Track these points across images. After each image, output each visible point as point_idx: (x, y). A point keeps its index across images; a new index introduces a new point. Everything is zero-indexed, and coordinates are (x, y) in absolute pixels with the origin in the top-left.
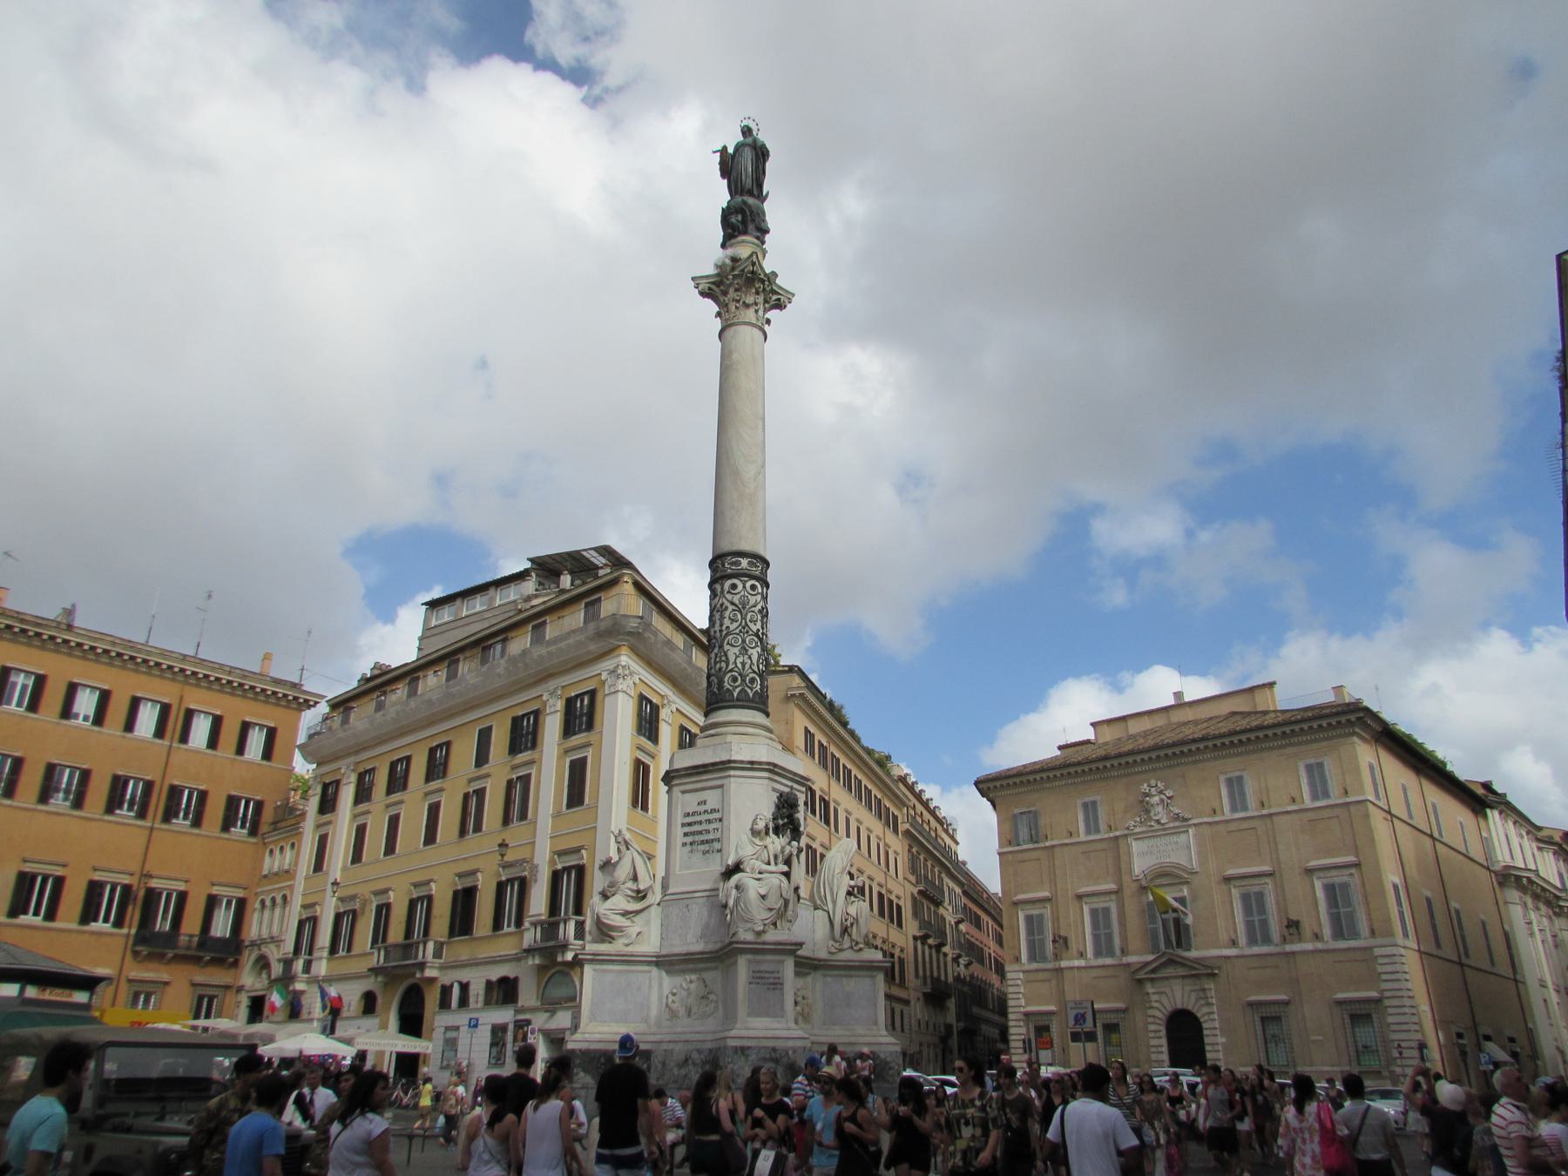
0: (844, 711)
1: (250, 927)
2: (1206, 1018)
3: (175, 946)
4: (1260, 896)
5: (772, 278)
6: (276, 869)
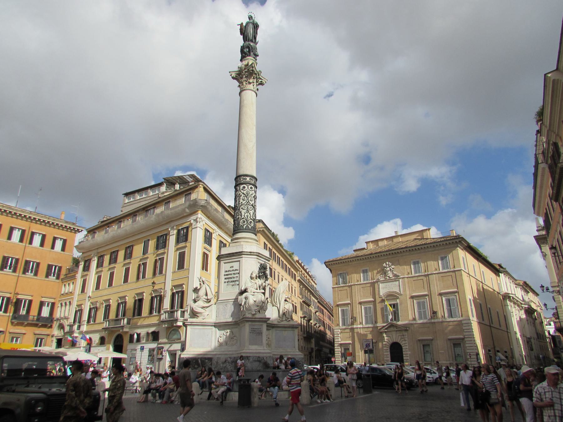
0: (278, 237)
1: (57, 313)
2: (404, 345)
3: (27, 320)
5: (259, 73)
6: (66, 292)
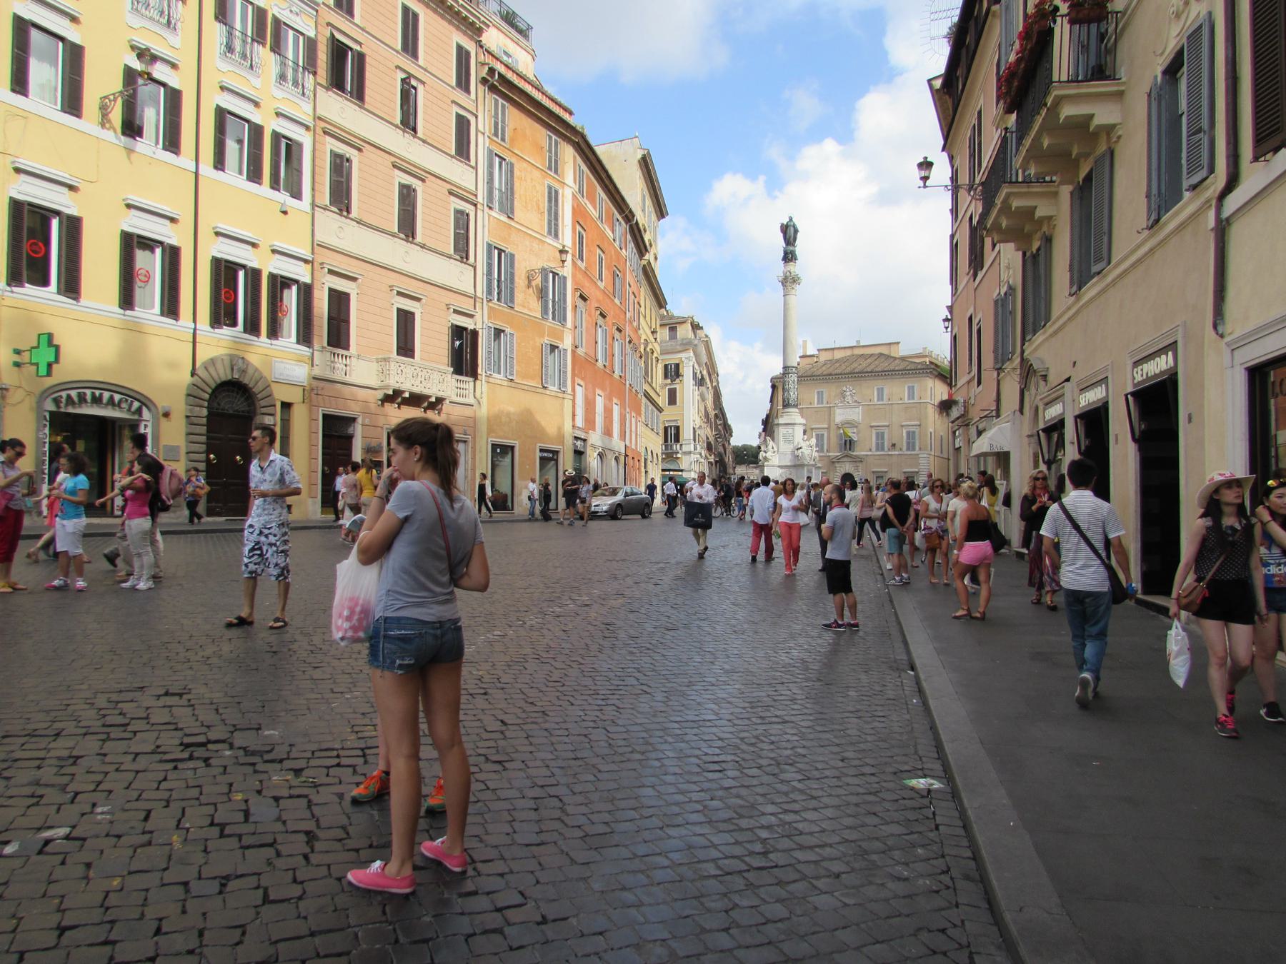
4: (883, 433)
